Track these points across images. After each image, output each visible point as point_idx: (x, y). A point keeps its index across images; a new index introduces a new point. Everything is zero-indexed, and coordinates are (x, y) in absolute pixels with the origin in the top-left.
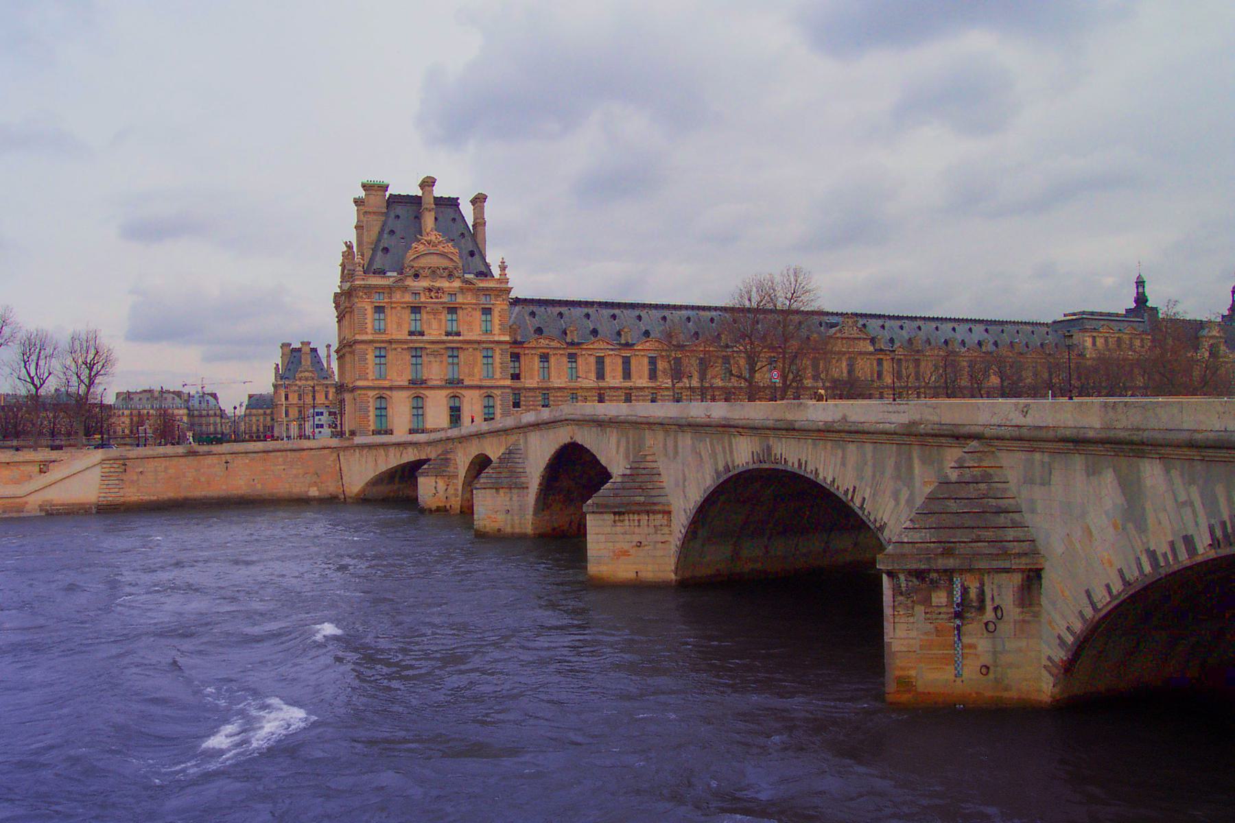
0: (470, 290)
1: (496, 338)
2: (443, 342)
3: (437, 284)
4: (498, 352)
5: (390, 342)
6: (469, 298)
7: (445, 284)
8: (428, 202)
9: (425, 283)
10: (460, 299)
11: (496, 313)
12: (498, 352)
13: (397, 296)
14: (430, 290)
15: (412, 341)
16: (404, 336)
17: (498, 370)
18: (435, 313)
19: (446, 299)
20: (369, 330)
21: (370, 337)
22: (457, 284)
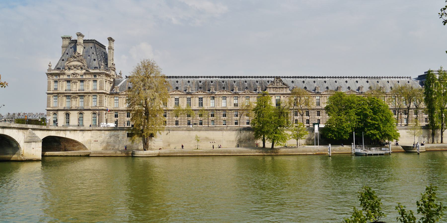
0: (88, 74)
1: (98, 91)
2: (77, 93)
3: (76, 72)
4: (98, 96)
5: (58, 93)
6: (87, 76)
7: (79, 72)
8: (81, 40)
9: (72, 72)
10: (84, 77)
11: (98, 82)
12: (98, 96)
13: (61, 77)
14: (74, 74)
15: (66, 93)
16: (63, 91)
17: (98, 104)
18: (75, 83)
19: (79, 77)
20: (52, 89)
21: (52, 92)
22: (84, 71)
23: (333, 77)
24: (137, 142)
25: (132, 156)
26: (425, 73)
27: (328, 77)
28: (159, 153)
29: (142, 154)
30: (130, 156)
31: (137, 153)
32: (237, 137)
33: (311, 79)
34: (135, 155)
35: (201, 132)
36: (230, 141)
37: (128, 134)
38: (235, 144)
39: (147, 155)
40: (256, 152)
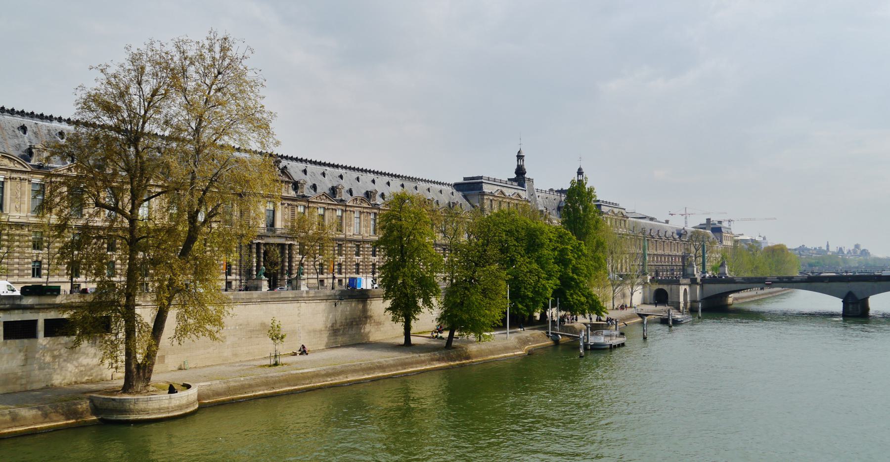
23: (350, 168)
24: (48, 359)
25: (104, 423)
26: (465, 179)
27: (342, 167)
28: (200, 397)
29: (167, 410)
30: (93, 424)
31: (142, 406)
32: (327, 318)
33: (313, 166)
34: (132, 417)
35: (251, 307)
36: (315, 331)
37: (7, 325)
38: (324, 339)
39: (180, 407)
40: (433, 360)
